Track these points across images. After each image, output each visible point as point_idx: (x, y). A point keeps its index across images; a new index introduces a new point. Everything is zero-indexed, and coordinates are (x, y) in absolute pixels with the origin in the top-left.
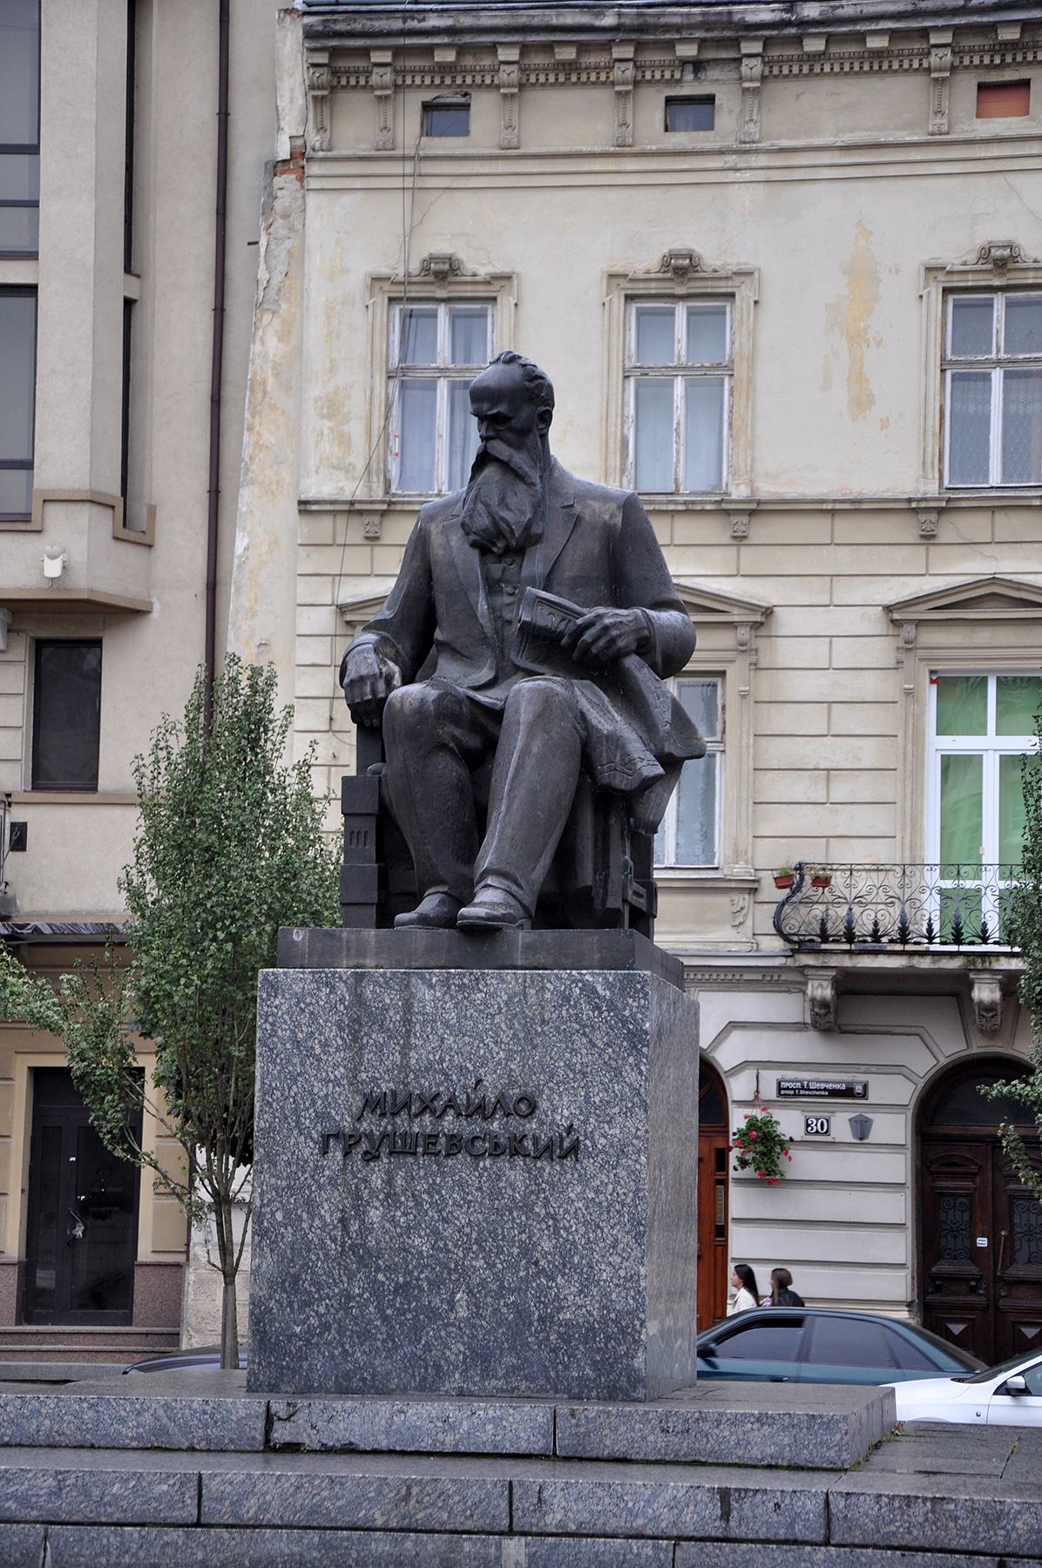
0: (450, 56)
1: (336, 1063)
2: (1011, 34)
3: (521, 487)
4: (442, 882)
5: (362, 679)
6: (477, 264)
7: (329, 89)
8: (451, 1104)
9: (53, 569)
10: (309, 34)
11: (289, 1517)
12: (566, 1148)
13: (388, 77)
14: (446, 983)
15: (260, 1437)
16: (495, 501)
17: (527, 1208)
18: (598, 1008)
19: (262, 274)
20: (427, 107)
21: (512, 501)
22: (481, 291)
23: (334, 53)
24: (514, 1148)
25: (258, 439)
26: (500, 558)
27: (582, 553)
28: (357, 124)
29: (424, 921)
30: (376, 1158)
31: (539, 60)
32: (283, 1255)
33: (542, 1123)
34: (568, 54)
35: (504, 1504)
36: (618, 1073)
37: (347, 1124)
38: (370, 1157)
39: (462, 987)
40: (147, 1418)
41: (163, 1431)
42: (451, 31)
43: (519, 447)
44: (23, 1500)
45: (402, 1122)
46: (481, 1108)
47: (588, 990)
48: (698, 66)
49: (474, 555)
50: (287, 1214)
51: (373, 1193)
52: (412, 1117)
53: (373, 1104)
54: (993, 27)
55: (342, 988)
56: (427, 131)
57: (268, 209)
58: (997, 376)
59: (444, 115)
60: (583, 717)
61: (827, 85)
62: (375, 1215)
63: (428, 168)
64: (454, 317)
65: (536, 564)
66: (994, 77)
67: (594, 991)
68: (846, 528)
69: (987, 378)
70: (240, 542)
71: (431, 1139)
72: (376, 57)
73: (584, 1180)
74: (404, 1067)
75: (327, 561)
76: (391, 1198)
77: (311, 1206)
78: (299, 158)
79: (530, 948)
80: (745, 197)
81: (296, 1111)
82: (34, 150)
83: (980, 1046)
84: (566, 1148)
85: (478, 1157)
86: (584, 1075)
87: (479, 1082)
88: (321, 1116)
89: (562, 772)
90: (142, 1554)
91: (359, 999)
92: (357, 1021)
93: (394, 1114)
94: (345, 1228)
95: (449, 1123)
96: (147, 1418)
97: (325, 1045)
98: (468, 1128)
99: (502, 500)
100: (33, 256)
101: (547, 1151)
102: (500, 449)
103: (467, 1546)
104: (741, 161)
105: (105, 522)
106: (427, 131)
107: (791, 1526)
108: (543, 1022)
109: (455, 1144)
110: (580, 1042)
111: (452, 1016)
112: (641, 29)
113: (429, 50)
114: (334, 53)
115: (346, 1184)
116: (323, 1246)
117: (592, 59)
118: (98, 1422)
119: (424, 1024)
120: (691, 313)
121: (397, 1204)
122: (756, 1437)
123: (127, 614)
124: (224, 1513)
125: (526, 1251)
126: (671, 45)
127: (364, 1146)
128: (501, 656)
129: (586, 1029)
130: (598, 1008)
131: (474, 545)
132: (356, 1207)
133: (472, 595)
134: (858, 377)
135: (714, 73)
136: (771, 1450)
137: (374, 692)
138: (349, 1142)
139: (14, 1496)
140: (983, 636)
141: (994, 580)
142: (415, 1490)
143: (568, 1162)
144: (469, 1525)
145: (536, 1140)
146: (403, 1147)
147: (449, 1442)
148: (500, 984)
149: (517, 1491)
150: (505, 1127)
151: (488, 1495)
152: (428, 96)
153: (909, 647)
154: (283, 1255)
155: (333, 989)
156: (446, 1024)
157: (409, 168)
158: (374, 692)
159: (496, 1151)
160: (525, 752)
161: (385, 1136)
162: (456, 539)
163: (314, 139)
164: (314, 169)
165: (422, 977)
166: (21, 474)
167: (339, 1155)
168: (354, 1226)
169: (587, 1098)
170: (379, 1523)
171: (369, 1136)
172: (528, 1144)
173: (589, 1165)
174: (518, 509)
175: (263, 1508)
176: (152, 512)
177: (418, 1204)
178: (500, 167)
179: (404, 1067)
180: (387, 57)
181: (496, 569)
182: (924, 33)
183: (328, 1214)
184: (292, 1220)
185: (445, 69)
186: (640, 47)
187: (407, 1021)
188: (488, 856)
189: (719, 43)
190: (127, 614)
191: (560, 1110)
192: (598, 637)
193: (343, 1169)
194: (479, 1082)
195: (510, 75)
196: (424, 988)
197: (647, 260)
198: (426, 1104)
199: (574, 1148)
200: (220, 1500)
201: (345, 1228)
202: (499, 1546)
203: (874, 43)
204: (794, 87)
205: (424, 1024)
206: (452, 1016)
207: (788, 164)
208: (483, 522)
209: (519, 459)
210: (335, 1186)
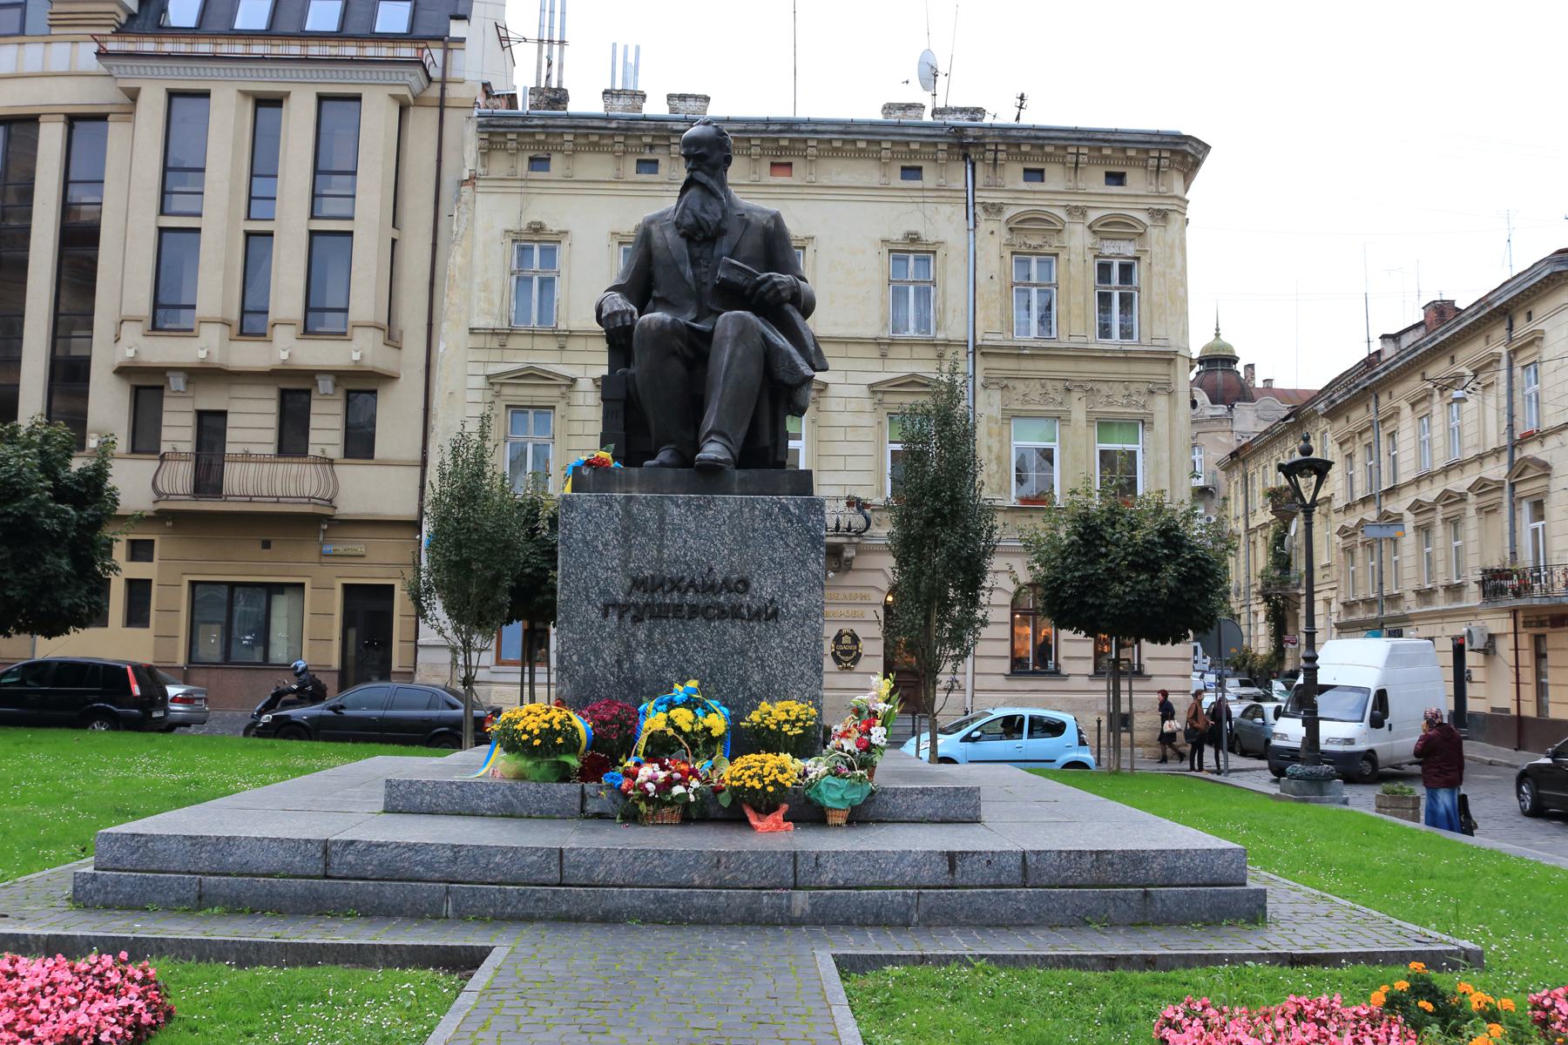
0: (542, 137)
1: (614, 557)
3: (713, 200)
4: (671, 442)
5: (615, 313)
6: (552, 225)
8: (692, 584)
9: (356, 356)
10: (480, 125)
11: (629, 879)
12: (769, 613)
13: (515, 145)
14: (688, 504)
15: (577, 809)
16: (697, 208)
17: (742, 653)
18: (790, 521)
19: (455, 228)
20: (531, 159)
21: (709, 208)
22: (554, 238)
23: (491, 134)
24: (735, 613)
25: (450, 300)
26: (699, 244)
27: (753, 241)
29: (662, 465)
30: (641, 620)
31: (582, 141)
32: (578, 684)
33: (753, 597)
35: (790, 868)
36: (804, 563)
37: (621, 598)
38: (637, 619)
39: (699, 507)
40: (498, 795)
41: (510, 804)
42: (543, 126)
43: (712, 176)
44: (429, 866)
45: (658, 597)
46: (712, 587)
47: (784, 509)
48: (651, 147)
49: (683, 243)
50: (580, 657)
51: (639, 643)
52: (665, 593)
53: (638, 583)
54: (777, 140)
55: (617, 507)
56: (532, 168)
57: (458, 200)
60: (764, 336)
62: (640, 658)
64: (542, 249)
65: (724, 245)
67: (788, 509)
70: (441, 347)
71: (678, 608)
72: (510, 136)
73: (781, 635)
74: (660, 560)
75: (482, 355)
76: (651, 646)
77: (597, 652)
78: (473, 179)
79: (743, 481)
81: (586, 589)
82: (354, 173)
84: (769, 613)
85: (710, 620)
86: (782, 565)
87: (711, 570)
88: (603, 592)
89: (755, 369)
90: (520, 906)
91: (628, 513)
92: (628, 528)
93: (653, 591)
94: (620, 667)
96: (498, 795)
97: (606, 545)
98: (702, 600)
99: (703, 208)
100: (352, 218)
101: (756, 615)
102: (701, 176)
103: (765, 899)
105: (380, 337)
106: (532, 168)
107: (998, 876)
108: (754, 530)
109: (694, 611)
110: (778, 543)
112: (628, 129)
113: (533, 134)
114: (491, 134)
115: (621, 637)
116: (605, 678)
117: (605, 141)
118: (463, 798)
119: (673, 531)
121: (655, 651)
122: (919, 803)
123: (389, 378)
124: (580, 876)
125: (743, 681)
126: (640, 137)
127: (633, 612)
128: (700, 304)
129: (783, 534)
130: (790, 521)
131: (682, 236)
132: (627, 653)
133: (681, 267)
135: (658, 150)
136: (930, 811)
137: (623, 321)
138: (622, 609)
139: (421, 863)
142: (724, 860)
143: (771, 623)
144: (764, 883)
145: (749, 607)
146: (659, 613)
148: (726, 503)
149: (801, 859)
150: (729, 599)
151: (779, 861)
154: (578, 684)
155: (611, 507)
156: (688, 531)
158: (623, 321)
159: (723, 614)
160: (732, 356)
161: (647, 605)
162: (670, 234)
163: (480, 170)
164: (480, 183)
165: (671, 499)
166: (342, 315)
167: (615, 618)
168: (626, 665)
169: (783, 581)
170: (697, 883)
171: (636, 605)
172: (745, 611)
173: (785, 625)
174: (712, 214)
175: (610, 873)
176: (401, 333)
177: (670, 651)
179: (660, 560)
181: (696, 251)
182: (749, 140)
184: (583, 661)
185: (539, 142)
186: (626, 137)
187: (661, 529)
188: (709, 421)
189: (661, 137)
190: (389, 378)
191: (765, 588)
192: (769, 290)
193: (619, 628)
194: (711, 570)
196: (673, 507)
198: (676, 584)
199: (775, 614)
200: (577, 867)
201: (620, 667)
202: (789, 897)
205: (673, 531)
208: (689, 220)
209: (713, 184)
210: (613, 638)
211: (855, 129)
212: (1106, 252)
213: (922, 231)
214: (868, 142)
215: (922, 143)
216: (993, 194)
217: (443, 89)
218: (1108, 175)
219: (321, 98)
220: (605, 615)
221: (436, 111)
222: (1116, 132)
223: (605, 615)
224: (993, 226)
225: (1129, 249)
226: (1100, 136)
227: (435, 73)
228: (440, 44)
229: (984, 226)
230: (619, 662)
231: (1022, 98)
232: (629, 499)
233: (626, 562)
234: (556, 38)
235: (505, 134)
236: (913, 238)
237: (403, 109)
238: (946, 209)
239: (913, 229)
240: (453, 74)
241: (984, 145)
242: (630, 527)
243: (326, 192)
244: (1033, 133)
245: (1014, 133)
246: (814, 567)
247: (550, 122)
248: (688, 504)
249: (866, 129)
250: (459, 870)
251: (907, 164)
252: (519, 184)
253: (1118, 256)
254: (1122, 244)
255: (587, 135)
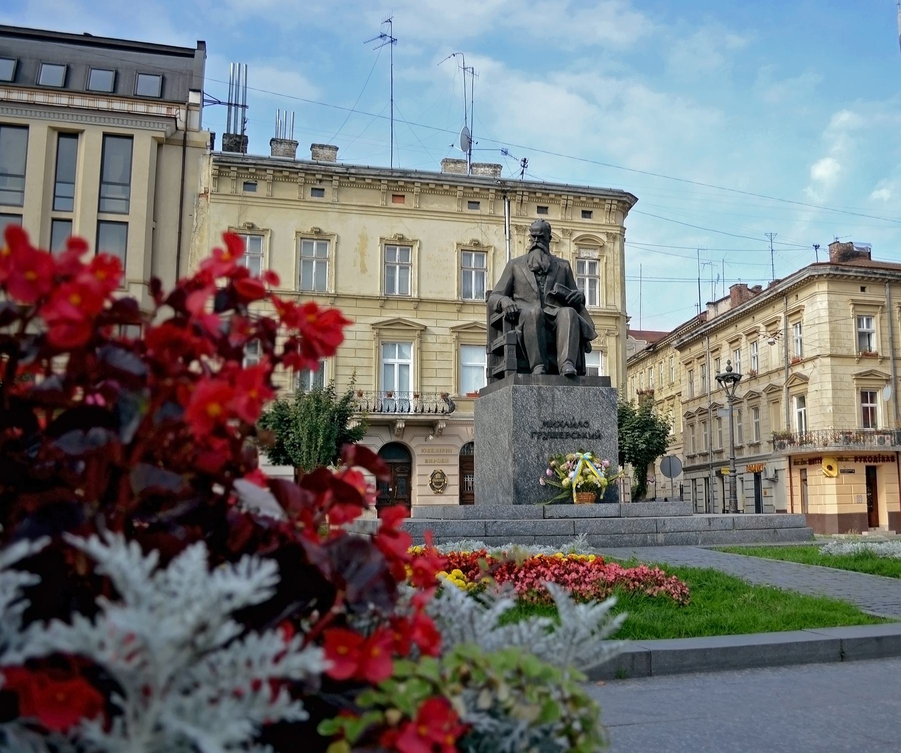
0: (254, 171)
1: (534, 412)
2: (402, 184)
6: (260, 225)
7: (218, 177)
14: (563, 390)
19: (195, 224)
20: (245, 183)
22: (260, 233)
23: (220, 166)
24: (584, 437)
28: (227, 187)
34: (287, 174)
38: (545, 439)
42: (255, 164)
44: (525, 530)
47: (601, 392)
53: (545, 424)
54: (397, 181)
58: (398, 267)
59: (250, 186)
61: (354, 190)
63: (248, 199)
66: (396, 193)
68: (359, 303)
69: (395, 268)
73: (602, 445)
74: (553, 414)
76: (551, 450)
80: (333, 215)
83: (394, 439)
85: (574, 438)
91: (539, 394)
95: (566, 429)
96: (510, 511)
98: (571, 431)
102: (540, 245)
104: (332, 206)
109: (568, 435)
111: (565, 399)
112: (307, 170)
113: (248, 169)
114: (220, 166)
117: (293, 176)
120: (318, 244)
121: (552, 452)
126: (314, 175)
129: (601, 403)
134: (363, 265)
135: (325, 183)
140: (396, 333)
141: (399, 319)
146: (554, 436)
147: (593, 514)
152: (246, 180)
153: (378, 335)
157: (240, 199)
159: (579, 436)
168: (541, 458)
173: (603, 441)
178: (266, 201)
179: (553, 414)
180: (236, 169)
181: (539, 278)
182: (380, 180)
183: (534, 455)
184: (523, 456)
185: (251, 174)
186: (306, 174)
189: (327, 176)
195: (270, 177)
197: (307, 229)
198: (561, 425)
203: (367, 181)
204: (346, 189)
206: (565, 399)
207: (344, 209)
209: (545, 248)
211: (443, 178)
212: (582, 256)
213: (480, 240)
214: (450, 186)
215: (481, 189)
216: (520, 220)
217: (185, 135)
218: (583, 212)
219: (106, 135)
220: (532, 437)
221: (181, 149)
222: (588, 188)
223: (532, 437)
224: (521, 238)
225: (596, 254)
226: (580, 190)
227: (181, 125)
228: (184, 107)
229: (516, 238)
230: (538, 457)
231: (525, 161)
232: (540, 388)
233: (539, 415)
234: (240, 103)
235: (229, 167)
236: (477, 244)
237: (160, 145)
238: (494, 227)
239: (475, 238)
240: (194, 125)
241: (516, 192)
242: (540, 400)
243: (107, 196)
244: (544, 187)
245: (533, 186)
246: (613, 416)
247: (260, 162)
248: (563, 390)
249: (449, 178)
250: (536, 531)
251: (472, 200)
252: (238, 198)
253: (588, 258)
254: (591, 252)
255: (281, 172)
